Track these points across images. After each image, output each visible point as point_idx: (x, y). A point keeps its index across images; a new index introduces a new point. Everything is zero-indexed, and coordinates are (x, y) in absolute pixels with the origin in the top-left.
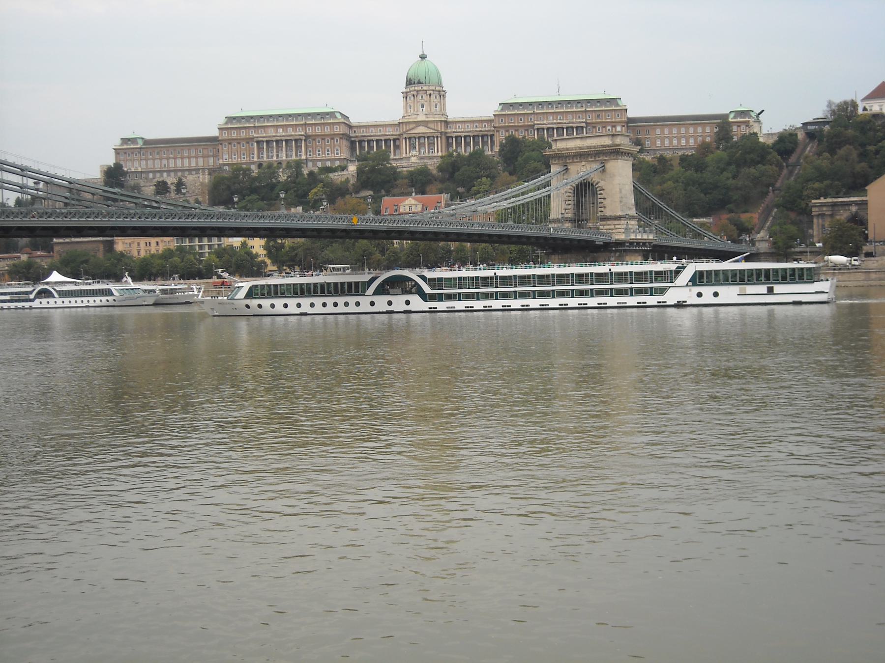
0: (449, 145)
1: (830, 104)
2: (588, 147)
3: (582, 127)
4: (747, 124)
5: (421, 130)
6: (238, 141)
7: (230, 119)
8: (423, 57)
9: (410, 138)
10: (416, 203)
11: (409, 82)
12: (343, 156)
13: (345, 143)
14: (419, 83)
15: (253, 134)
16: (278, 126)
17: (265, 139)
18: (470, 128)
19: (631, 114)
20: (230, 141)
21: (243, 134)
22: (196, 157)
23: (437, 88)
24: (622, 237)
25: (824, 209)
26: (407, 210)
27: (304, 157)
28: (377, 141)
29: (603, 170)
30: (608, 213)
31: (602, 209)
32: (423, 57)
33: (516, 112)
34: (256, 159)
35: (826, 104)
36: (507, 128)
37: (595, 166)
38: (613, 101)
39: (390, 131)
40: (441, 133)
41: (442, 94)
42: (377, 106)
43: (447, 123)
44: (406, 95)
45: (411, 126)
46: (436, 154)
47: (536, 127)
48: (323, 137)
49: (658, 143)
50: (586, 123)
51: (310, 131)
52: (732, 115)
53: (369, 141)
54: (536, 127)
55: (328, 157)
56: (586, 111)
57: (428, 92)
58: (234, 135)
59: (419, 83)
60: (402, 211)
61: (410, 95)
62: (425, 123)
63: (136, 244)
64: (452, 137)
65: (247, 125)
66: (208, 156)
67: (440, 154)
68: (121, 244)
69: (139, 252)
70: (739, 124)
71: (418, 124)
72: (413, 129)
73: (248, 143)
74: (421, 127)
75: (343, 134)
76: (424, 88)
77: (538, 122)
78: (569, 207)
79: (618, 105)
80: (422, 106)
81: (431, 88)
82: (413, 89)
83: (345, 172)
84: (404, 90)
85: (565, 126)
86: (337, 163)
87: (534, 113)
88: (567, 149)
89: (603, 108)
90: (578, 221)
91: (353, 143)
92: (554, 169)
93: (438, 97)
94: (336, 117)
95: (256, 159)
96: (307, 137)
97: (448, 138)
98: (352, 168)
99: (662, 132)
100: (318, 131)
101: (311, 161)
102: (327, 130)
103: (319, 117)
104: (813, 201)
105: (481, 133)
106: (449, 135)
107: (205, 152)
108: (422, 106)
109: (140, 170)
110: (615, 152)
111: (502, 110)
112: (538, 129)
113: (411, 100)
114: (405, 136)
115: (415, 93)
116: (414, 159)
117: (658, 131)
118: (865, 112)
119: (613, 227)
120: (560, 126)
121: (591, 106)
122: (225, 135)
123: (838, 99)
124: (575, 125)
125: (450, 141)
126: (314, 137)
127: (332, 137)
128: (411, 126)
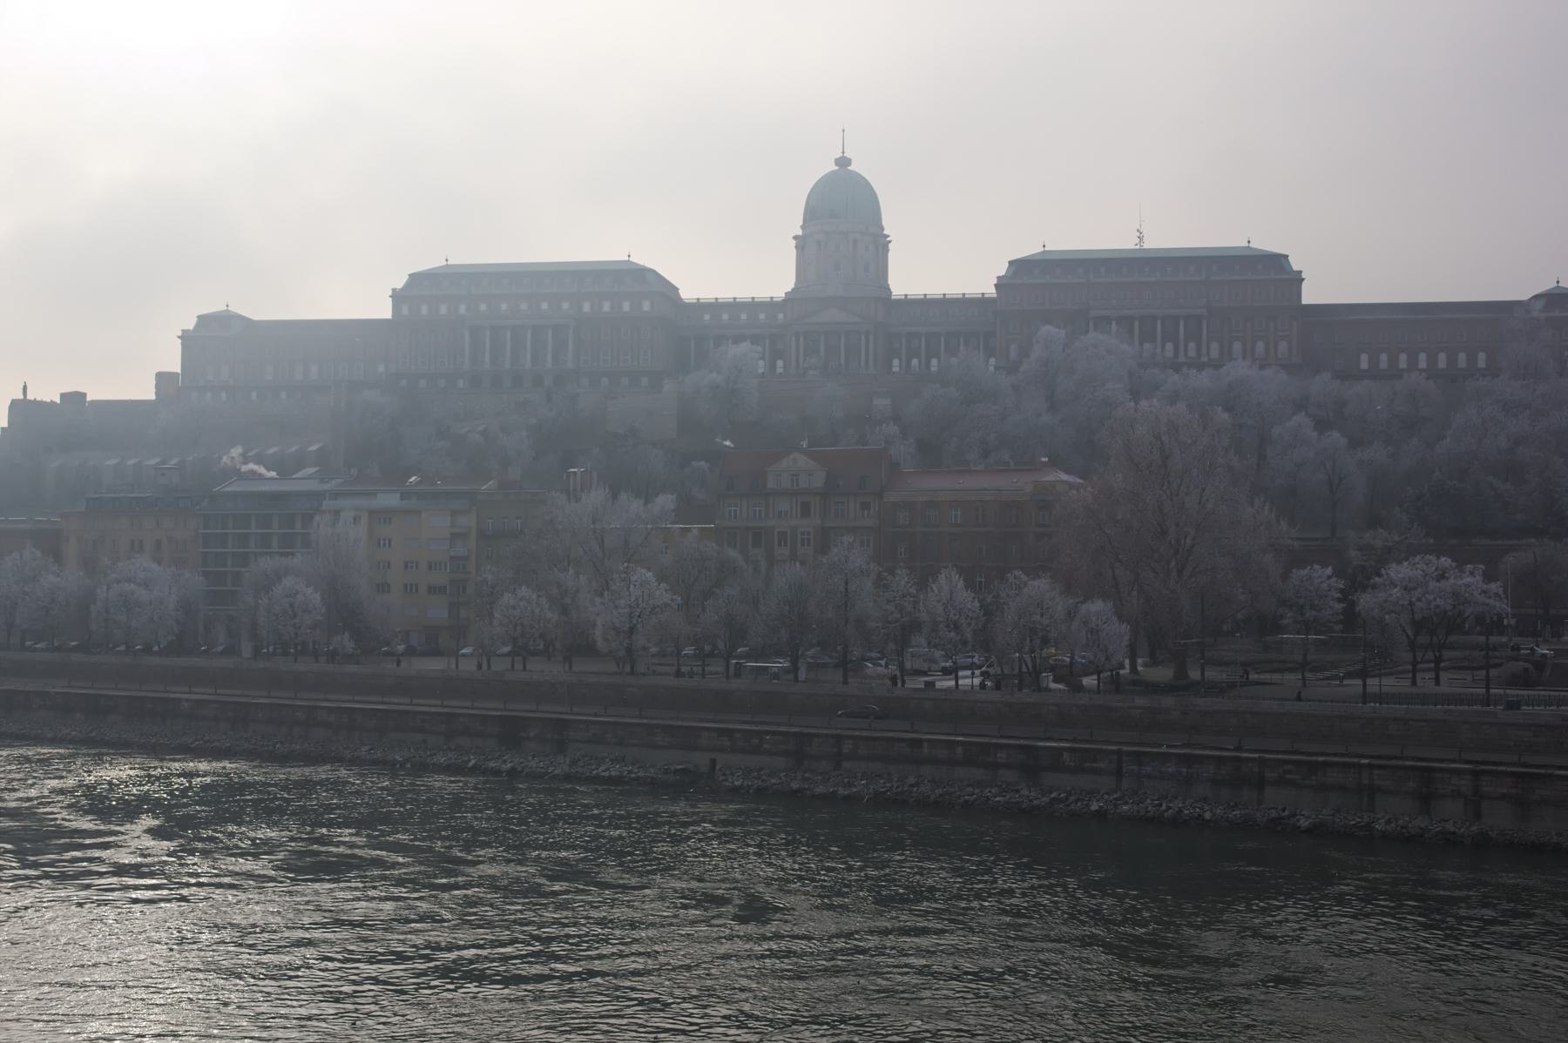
8: (843, 162)
11: (813, 213)
19: (1311, 295)
32: (843, 162)
38: (1278, 262)
42: (736, 261)
49: (1364, 365)
52: (1539, 304)
60: (771, 485)
84: (800, 233)
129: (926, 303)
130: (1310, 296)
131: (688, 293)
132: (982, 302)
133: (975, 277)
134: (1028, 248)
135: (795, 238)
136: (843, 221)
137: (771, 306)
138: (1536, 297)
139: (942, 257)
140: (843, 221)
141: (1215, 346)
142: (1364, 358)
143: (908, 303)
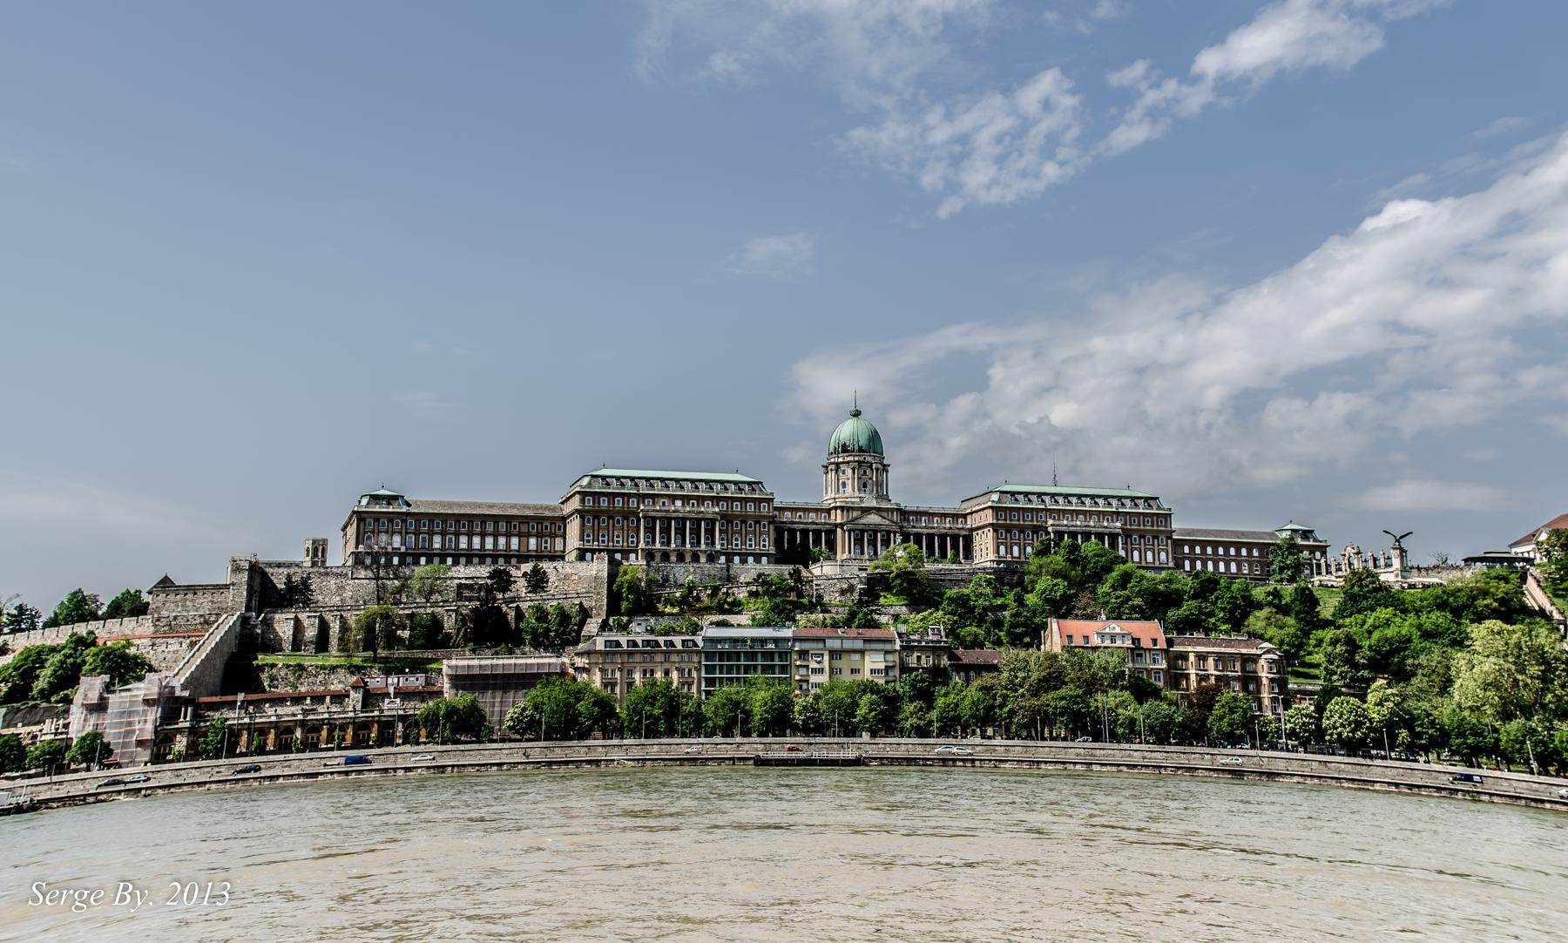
5: (873, 519)
15: (633, 503)
22: (508, 535)
26: (1107, 643)
27: (718, 547)
41: (885, 468)
45: (855, 514)
56: (1118, 513)
62: (878, 510)
66: (529, 535)
71: (866, 511)
80: (865, 485)
87: (1047, 510)
91: (779, 531)
96: (723, 516)
99: (1192, 549)
100: (737, 507)
107: (524, 529)
109: (403, 549)
117: (1186, 549)
128: (855, 514)
142: (1187, 563)
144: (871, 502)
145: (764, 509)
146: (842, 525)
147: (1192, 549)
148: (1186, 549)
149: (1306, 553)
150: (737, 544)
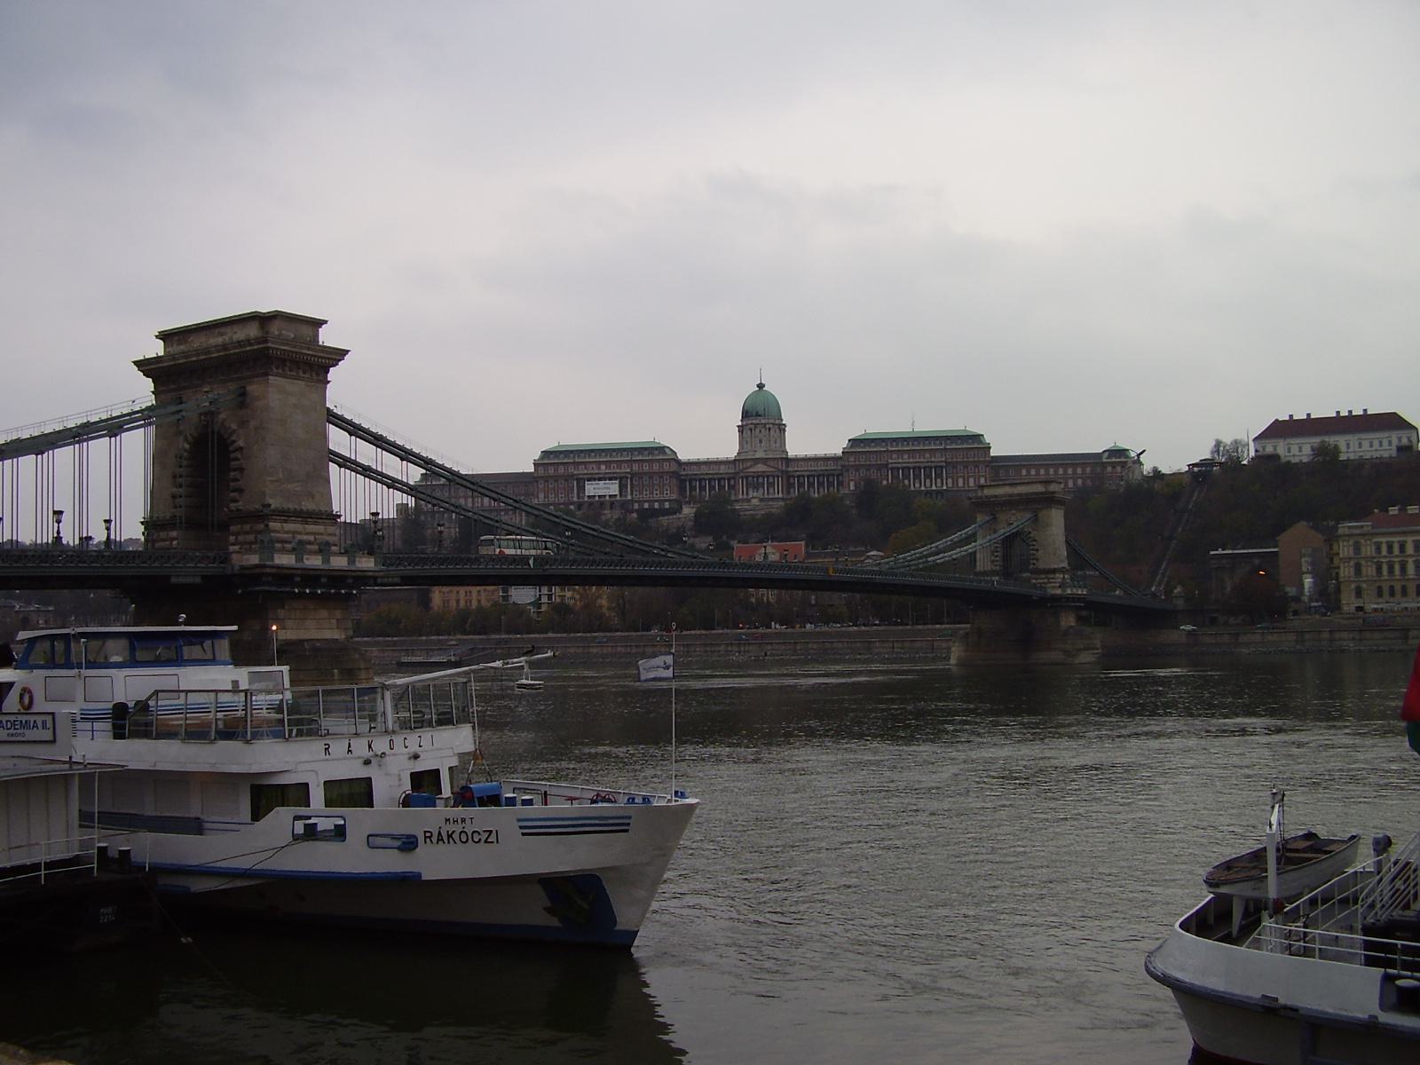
0: (790, 486)
1: (1218, 443)
2: (1019, 495)
3: (942, 467)
4: (1123, 465)
5: (760, 468)
6: (556, 478)
7: (546, 454)
8: (761, 386)
9: (747, 477)
10: (774, 551)
11: (746, 414)
12: (674, 496)
13: (674, 481)
14: (758, 415)
15: (571, 470)
16: (600, 463)
17: (586, 477)
18: (813, 467)
19: (993, 453)
20: (546, 479)
21: (561, 470)
23: (777, 422)
24: (1059, 592)
25: (1224, 561)
27: (629, 497)
28: (710, 480)
29: (1035, 519)
30: (1041, 565)
31: (1035, 561)
32: (761, 386)
33: (867, 449)
34: (575, 499)
35: (1214, 443)
36: (857, 468)
37: (1028, 515)
38: (977, 438)
39: (723, 469)
40: (783, 471)
41: (781, 428)
42: (709, 437)
43: (788, 460)
44: (741, 429)
45: (749, 464)
46: (776, 496)
47: (890, 466)
48: (651, 475)
50: (946, 462)
51: (635, 467)
52: (1106, 454)
53: (700, 480)
54: (890, 466)
55: (656, 498)
56: (945, 449)
57: (767, 426)
58: (551, 471)
59: (758, 415)
61: (747, 428)
62: (764, 461)
63: (455, 592)
64: (794, 477)
65: (566, 461)
67: (781, 495)
68: (438, 595)
69: (458, 601)
70: (1114, 465)
71: (757, 461)
72: (751, 466)
73: (566, 480)
74: (759, 465)
75: (673, 472)
76: (763, 421)
77: (894, 460)
78: (997, 559)
79: (981, 442)
80: (761, 442)
81: (770, 421)
82: (750, 422)
83: (678, 515)
85: (922, 465)
86: (667, 505)
87: (888, 451)
88: (996, 496)
89: (965, 446)
90: (1006, 573)
92: (981, 518)
93: (777, 430)
94: (665, 453)
95: (575, 499)
96: (633, 475)
97: (789, 477)
98: (688, 511)
100: (646, 468)
101: (636, 501)
102: (656, 467)
103: (646, 452)
104: (1212, 553)
105: (826, 473)
106: (791, 474)
108: (761, 442)
110: (1049, 500)
111: (851, 447)
112: (892, 469)
113: (747, 433)
114: (742, 474)
115: (753, 426)
116: (755, 501)
117: (1024, 472)
118: (1258, 454)
119: (1046, 580)
120: (917, 465)
121: (951, 443)
122: (541, 471)
123: (1227, 439)
124: (933, 465)
125: (792, 480)
126: (640, 475)
127: (661, 475)
128: (749, 464)
129: (807, 460)
130: (993, 453)
131: (683, 456)
132: (835, 459)
133: (832, 444)
134: (856, 433)
135: (738, 426)
136: (760, 418)
137: (726, 462)
138: (1104, 451)
139: (813, 435)
140: (760, 418)
141: (950, 481)
143: (797, 460)
144: (760, 454)
145: (666, 467)
146: (738, 473)
147: (1028, 472)
148: (1024, 472)
149: (1119, 469)
150: (646, 495)
